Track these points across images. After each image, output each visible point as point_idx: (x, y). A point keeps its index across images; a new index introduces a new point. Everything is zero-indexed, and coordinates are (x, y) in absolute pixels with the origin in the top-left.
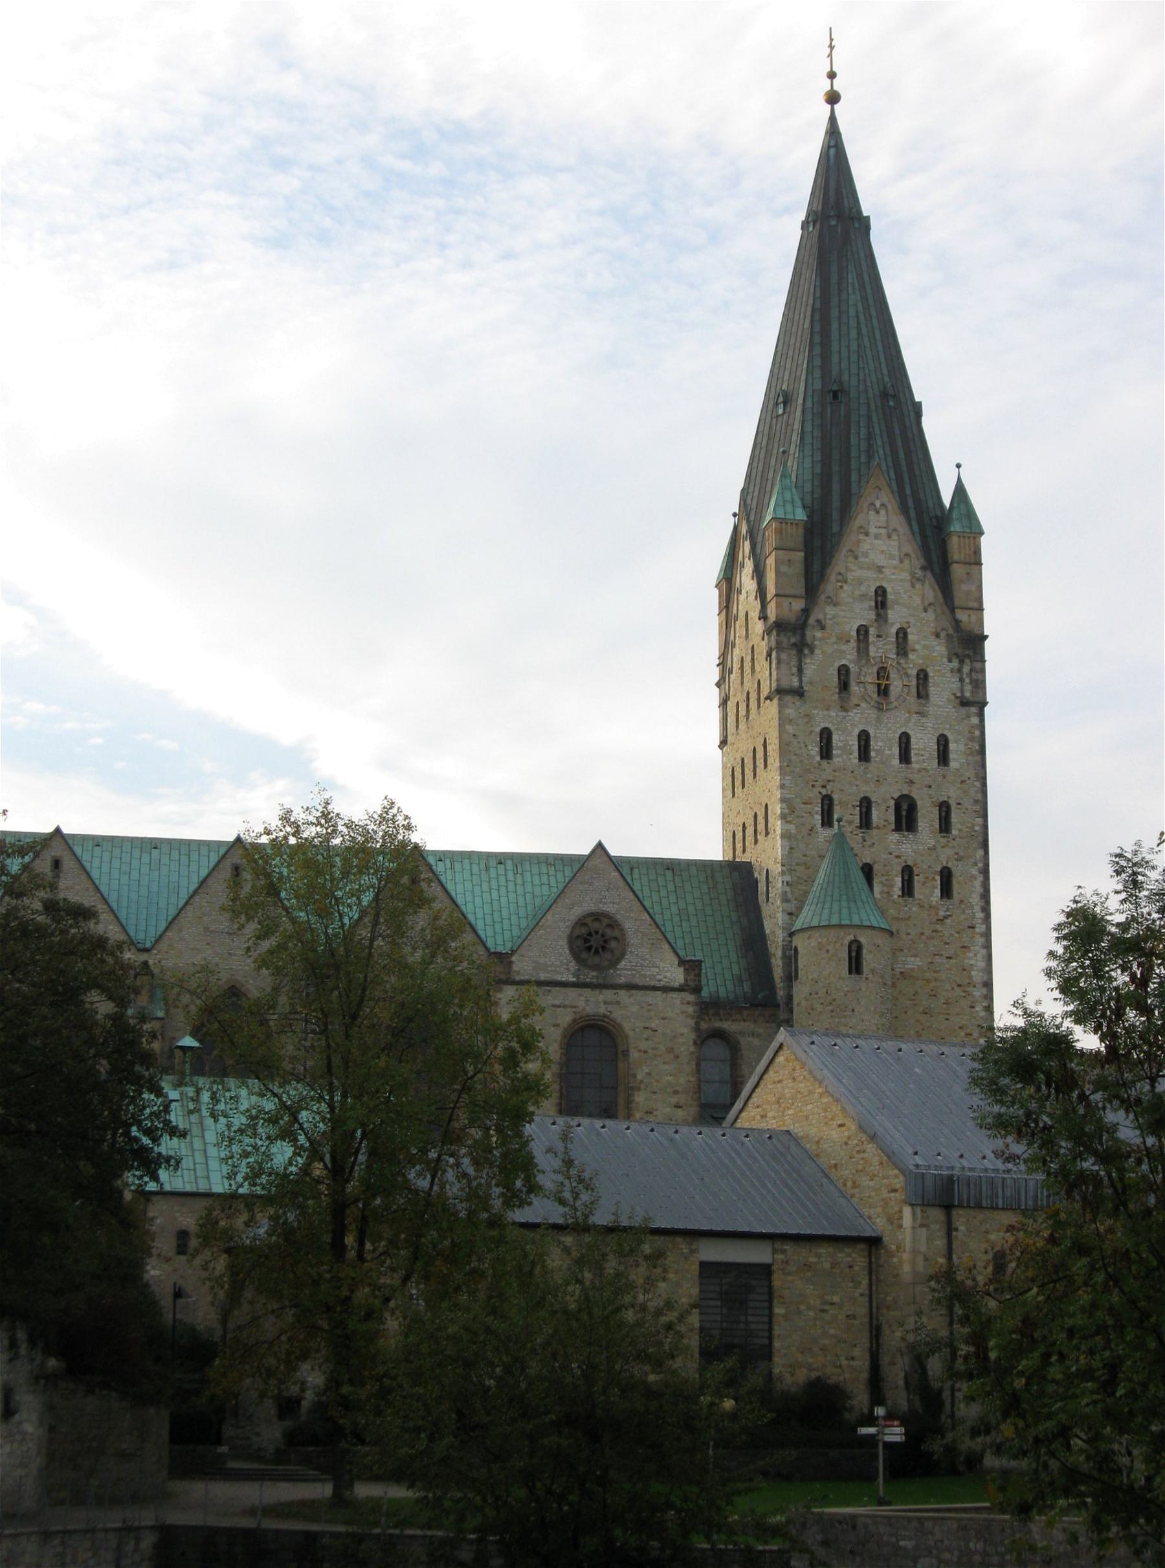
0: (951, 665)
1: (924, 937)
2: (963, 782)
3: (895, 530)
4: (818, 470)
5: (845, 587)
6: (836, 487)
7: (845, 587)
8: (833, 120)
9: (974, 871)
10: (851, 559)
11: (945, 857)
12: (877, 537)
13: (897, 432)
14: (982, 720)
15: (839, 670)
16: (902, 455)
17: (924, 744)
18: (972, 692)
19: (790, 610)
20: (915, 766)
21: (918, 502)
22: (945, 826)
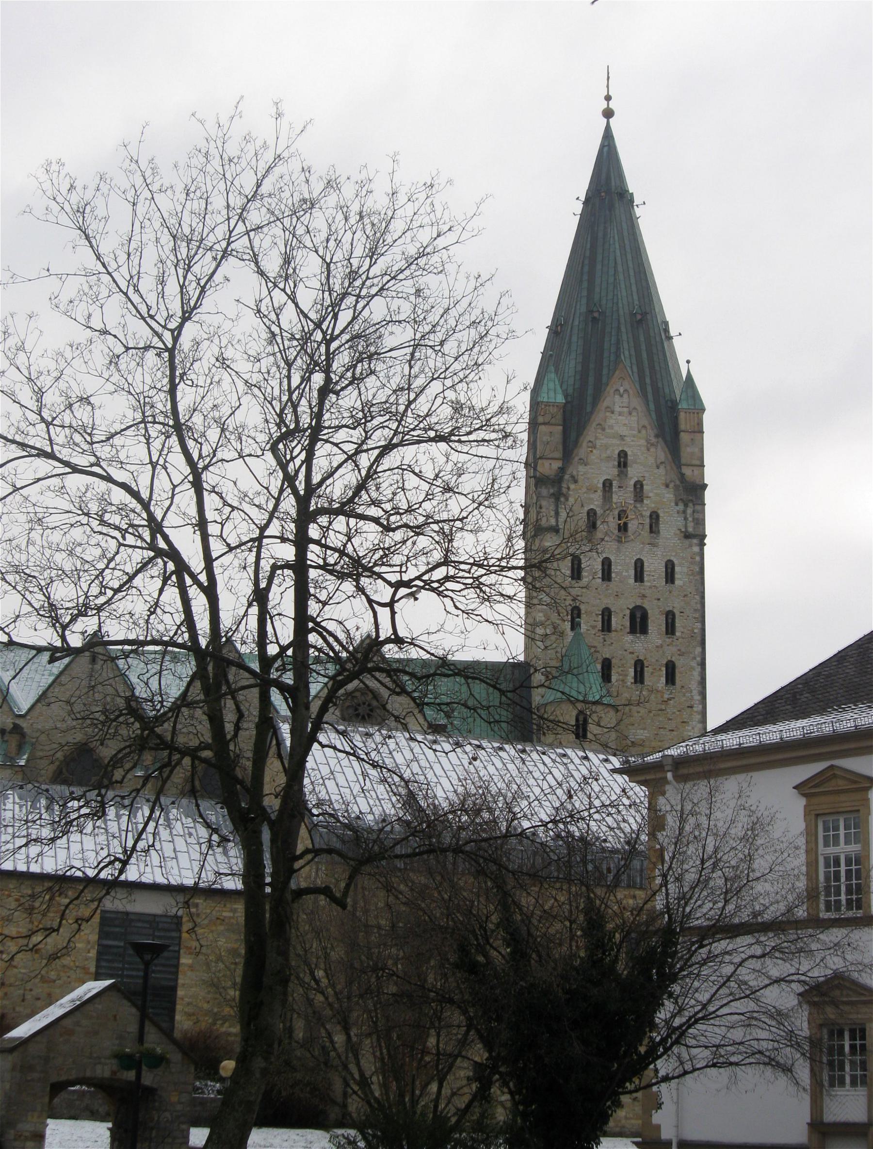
0: (678, 508)
1: (651, 715)
2: (685, 596)
3: (635, 408)
4: (579, 368)
5: (594, 451)
6: (591, 380)
7: (594, 451)
8: (608, 129)
9: (694, 664)
10: (599, 431)
11: (670, 653)
12: (620, 414)
13: (642, 339)
14: (702, 550)
15: (588, 513)
16: (644, 355)
17: (654, 567)
18: (694, 528)
19: (550, 469)
20: (646, 584)
21: (656, 391)
22: (670, 629)
